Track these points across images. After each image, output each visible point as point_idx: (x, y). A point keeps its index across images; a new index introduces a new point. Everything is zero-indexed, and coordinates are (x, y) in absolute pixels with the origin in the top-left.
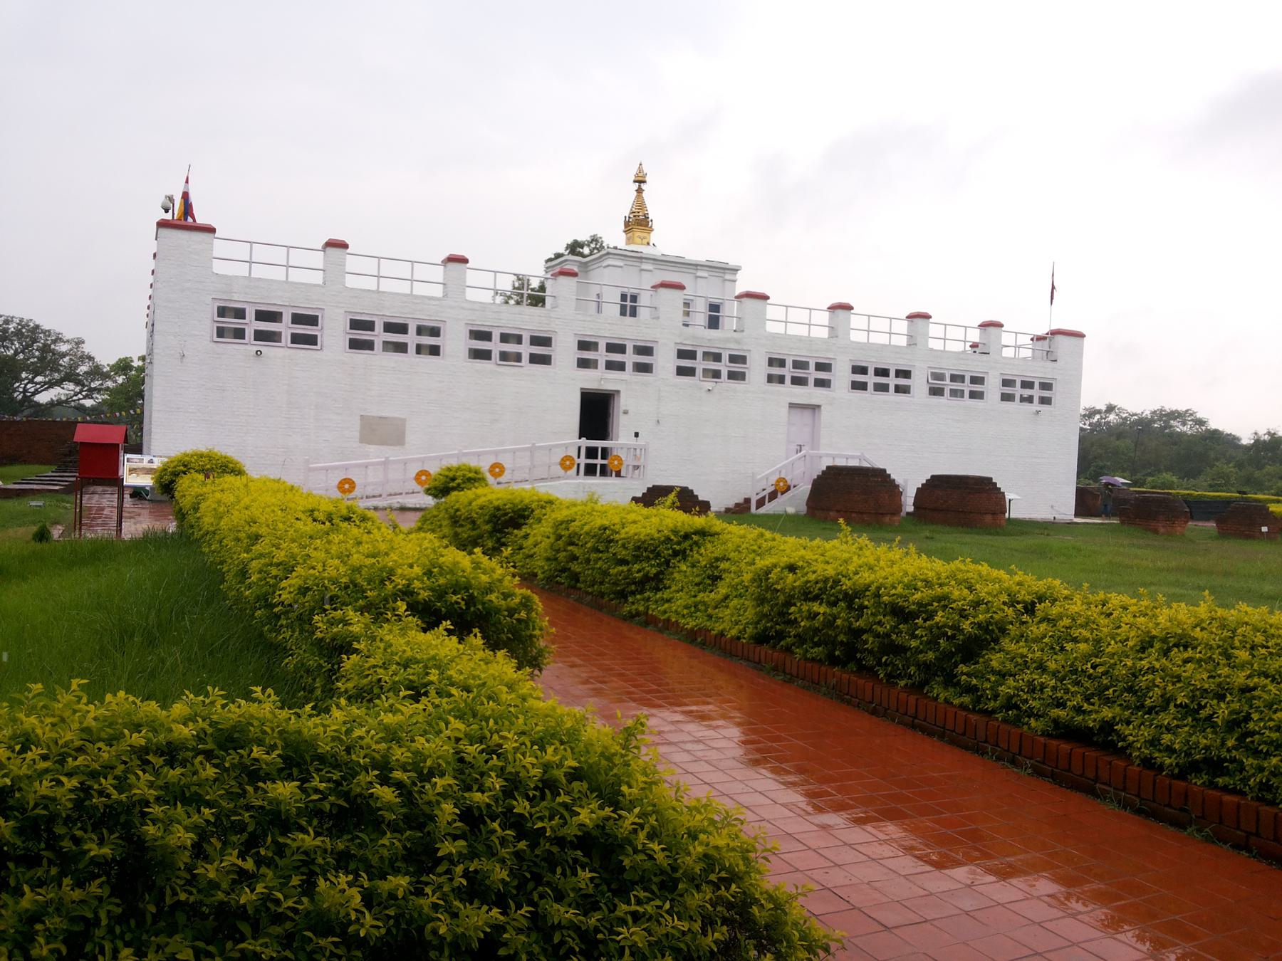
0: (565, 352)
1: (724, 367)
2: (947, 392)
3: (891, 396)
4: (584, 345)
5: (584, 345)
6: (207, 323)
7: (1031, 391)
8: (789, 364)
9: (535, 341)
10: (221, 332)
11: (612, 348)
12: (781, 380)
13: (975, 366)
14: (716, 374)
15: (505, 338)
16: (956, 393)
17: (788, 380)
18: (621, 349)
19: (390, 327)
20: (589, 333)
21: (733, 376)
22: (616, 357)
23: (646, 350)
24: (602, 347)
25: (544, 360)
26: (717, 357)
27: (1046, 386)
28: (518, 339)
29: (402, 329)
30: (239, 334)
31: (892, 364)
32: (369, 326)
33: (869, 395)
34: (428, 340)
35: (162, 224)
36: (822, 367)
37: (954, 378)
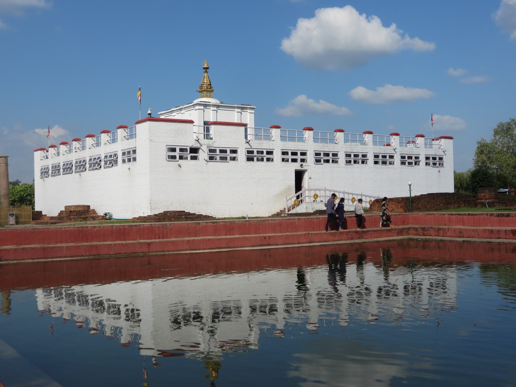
0: (277, 156)
1: (330, 158)
2: (407, 163)
4: (284, 153)
5: (284, 153)
6: (164, 153)
7: (435, 161)
8: (352, 156)
10: (169, 156)
12: (350, 162)
14: (327, 161)
15: (258, 152)
16: (410, 164)
17: (352, 162)
19: (222, 151)
21: (333, 161)
22: (294, 157)
23: (303, 154)
24: (290, 154)
26: (328, 155)
27: (441, 159)
28: (262, 153)
29: (225, 151)
30: (174, 157)
32: (214, 151)
34: (234, 155)
36: (364, 156)
37: (410, 158)
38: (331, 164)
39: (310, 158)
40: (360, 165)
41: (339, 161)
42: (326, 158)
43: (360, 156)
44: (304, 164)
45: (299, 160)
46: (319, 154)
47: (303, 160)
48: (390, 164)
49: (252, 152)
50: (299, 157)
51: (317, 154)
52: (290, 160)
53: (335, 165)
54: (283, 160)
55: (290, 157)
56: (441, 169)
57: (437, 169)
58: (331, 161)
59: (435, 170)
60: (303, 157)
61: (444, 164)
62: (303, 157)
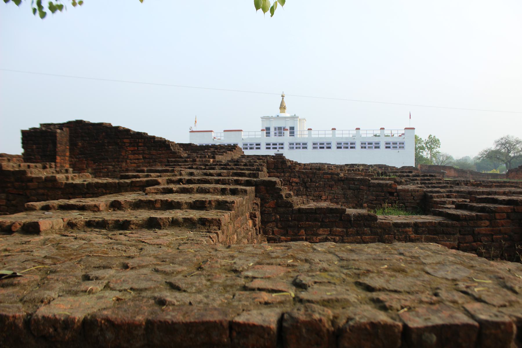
3: (349, 150)
9: (257, 145)
11: (273, 144)
13: (376, 140)
14: (300, 148)
15: (250, 145)
18: (276, 144)
20: (268, 142)
21: (303, 148)
24: (271, 144)
25: (259, 148)
31: (349, 141)
33: (342, 150)
35: (190, 132)
36: (328, 144)
37: (369, 144)
38: (301, 150)
39: (286, 146)
40: (325, 150)
41: (308, 147)
42: (298, 146)
43: (325, 144)
44: (280, 150)
45: (278, 148)
46: (293, 144)
47: (282, 148)
48: (351, 148)
49: (247, 145)
50: (278, 146)
51: (290, 144)
52: (271, 148)
53: (305, 150)
54: (267, 148)
55: (271, 146)
56: (401, 150)
57: (398, 150)
58: (301, 148)
59: (395, 151)
60: (282, 146)
61: (406, 147)
62: (282, 146)
